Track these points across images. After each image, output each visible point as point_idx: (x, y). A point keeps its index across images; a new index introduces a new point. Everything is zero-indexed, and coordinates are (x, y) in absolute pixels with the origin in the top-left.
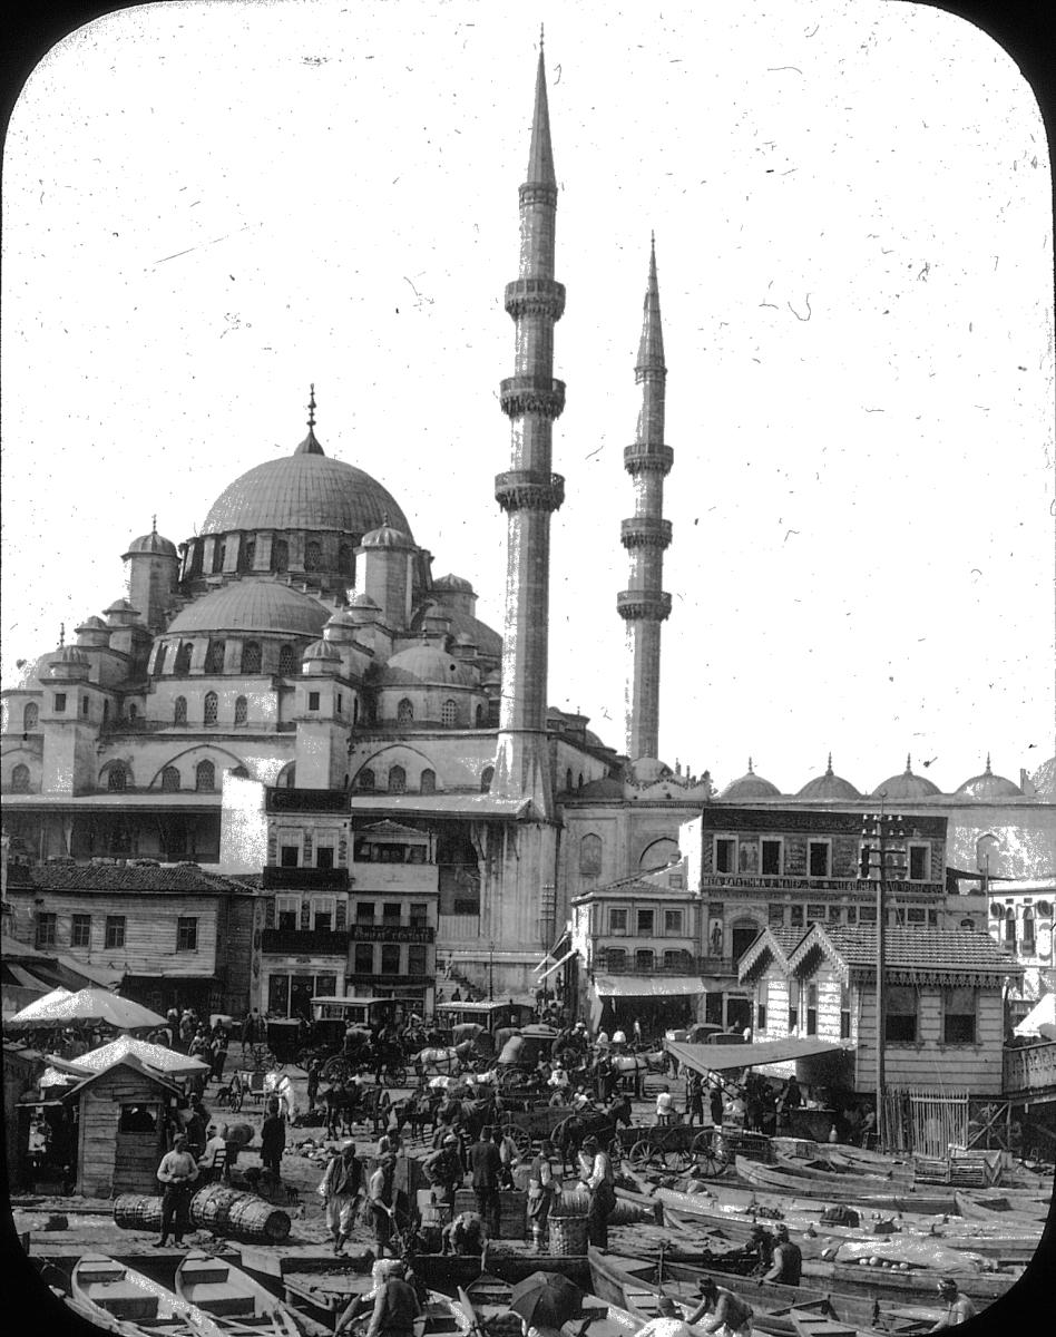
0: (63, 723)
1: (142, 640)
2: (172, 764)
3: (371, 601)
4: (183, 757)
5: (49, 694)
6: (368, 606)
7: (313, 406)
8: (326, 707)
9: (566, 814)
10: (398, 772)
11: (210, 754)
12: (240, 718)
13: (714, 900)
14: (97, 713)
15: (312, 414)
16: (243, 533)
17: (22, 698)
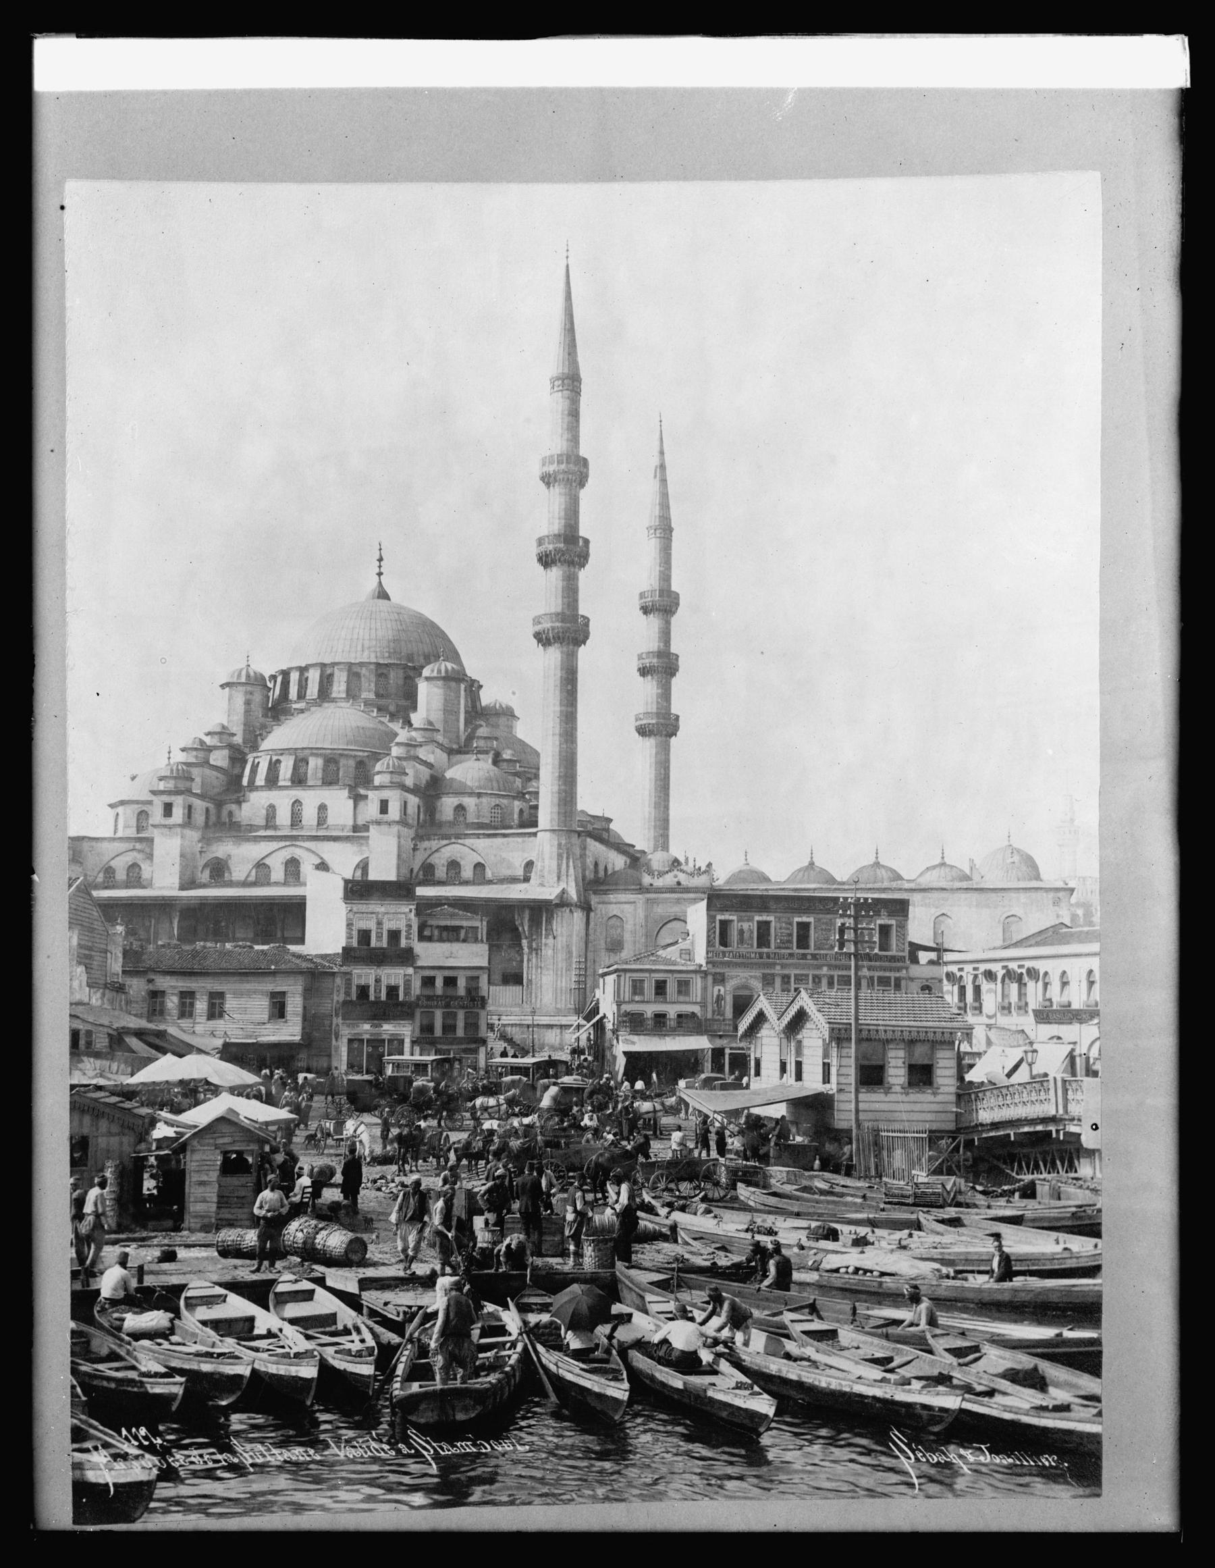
0: (170, 827)
1: (238, 757)
2: (267, 861)
3: (430, 723)
4: (274, 854)
5: (159, 802)
6: (430, 728)
7: (380, 560)
8: (394, 812)
9: (594, 900)
10: (454, 865)
11: (298, 853)
12: (321, 821)
13: (718, 970)
14: (199, 818)
15: (380, 567)
16: (323, 666)
17: (136, 806)
